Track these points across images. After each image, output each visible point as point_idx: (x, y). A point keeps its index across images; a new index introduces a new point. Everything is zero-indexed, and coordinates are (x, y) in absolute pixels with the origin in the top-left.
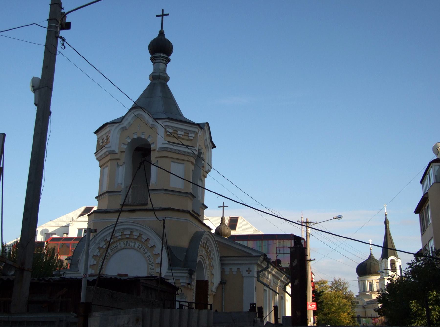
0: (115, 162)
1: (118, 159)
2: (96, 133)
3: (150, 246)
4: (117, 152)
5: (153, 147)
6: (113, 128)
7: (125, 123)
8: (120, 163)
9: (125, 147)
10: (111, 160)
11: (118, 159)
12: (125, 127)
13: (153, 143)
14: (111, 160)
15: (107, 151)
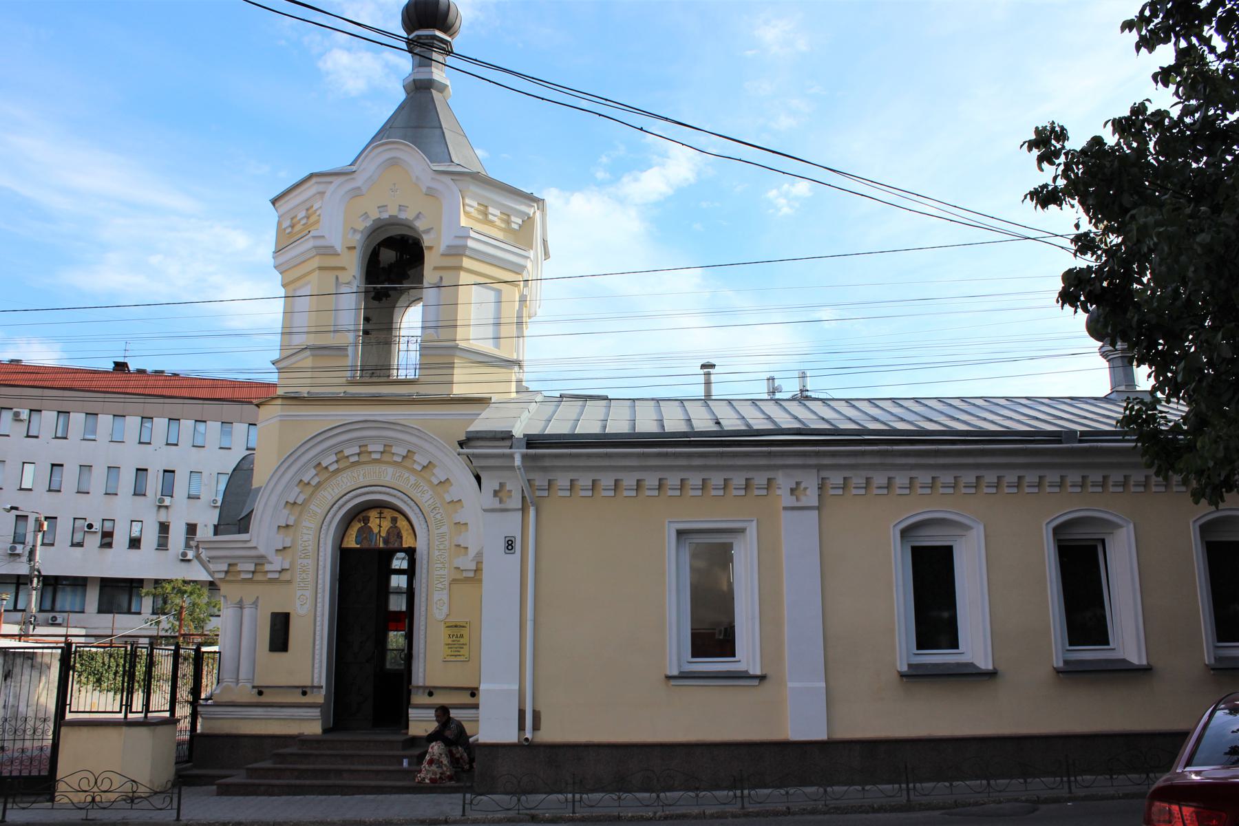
0: (331, 276)
1: (343, 269)
2: (274, 202)
3: (436, 482)
4: (339, 249)
5: (427, 241)
6: (332, 188)
7: (359, 181)
8: (345, 277)
9: (358, 237)
10: (320, 268)
11: (343, 269)
12: (359, 188)
13: (428, 231)
14: (320, 268)
15: (315, 247)
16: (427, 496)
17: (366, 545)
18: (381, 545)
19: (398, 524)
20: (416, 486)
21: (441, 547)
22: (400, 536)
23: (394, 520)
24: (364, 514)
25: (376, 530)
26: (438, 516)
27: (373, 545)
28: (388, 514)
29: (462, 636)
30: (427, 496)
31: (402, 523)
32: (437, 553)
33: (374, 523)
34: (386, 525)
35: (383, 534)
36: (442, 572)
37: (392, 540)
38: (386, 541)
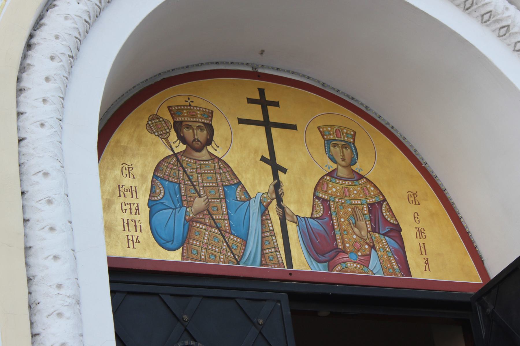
17: (212, 254)
18: (302, 262)
19: (362, 165)
24: (177, 96)
25: (257, 182)
27: (251, 260)
35: (300, 202)
37: (352, 234)
38: (322, 245)
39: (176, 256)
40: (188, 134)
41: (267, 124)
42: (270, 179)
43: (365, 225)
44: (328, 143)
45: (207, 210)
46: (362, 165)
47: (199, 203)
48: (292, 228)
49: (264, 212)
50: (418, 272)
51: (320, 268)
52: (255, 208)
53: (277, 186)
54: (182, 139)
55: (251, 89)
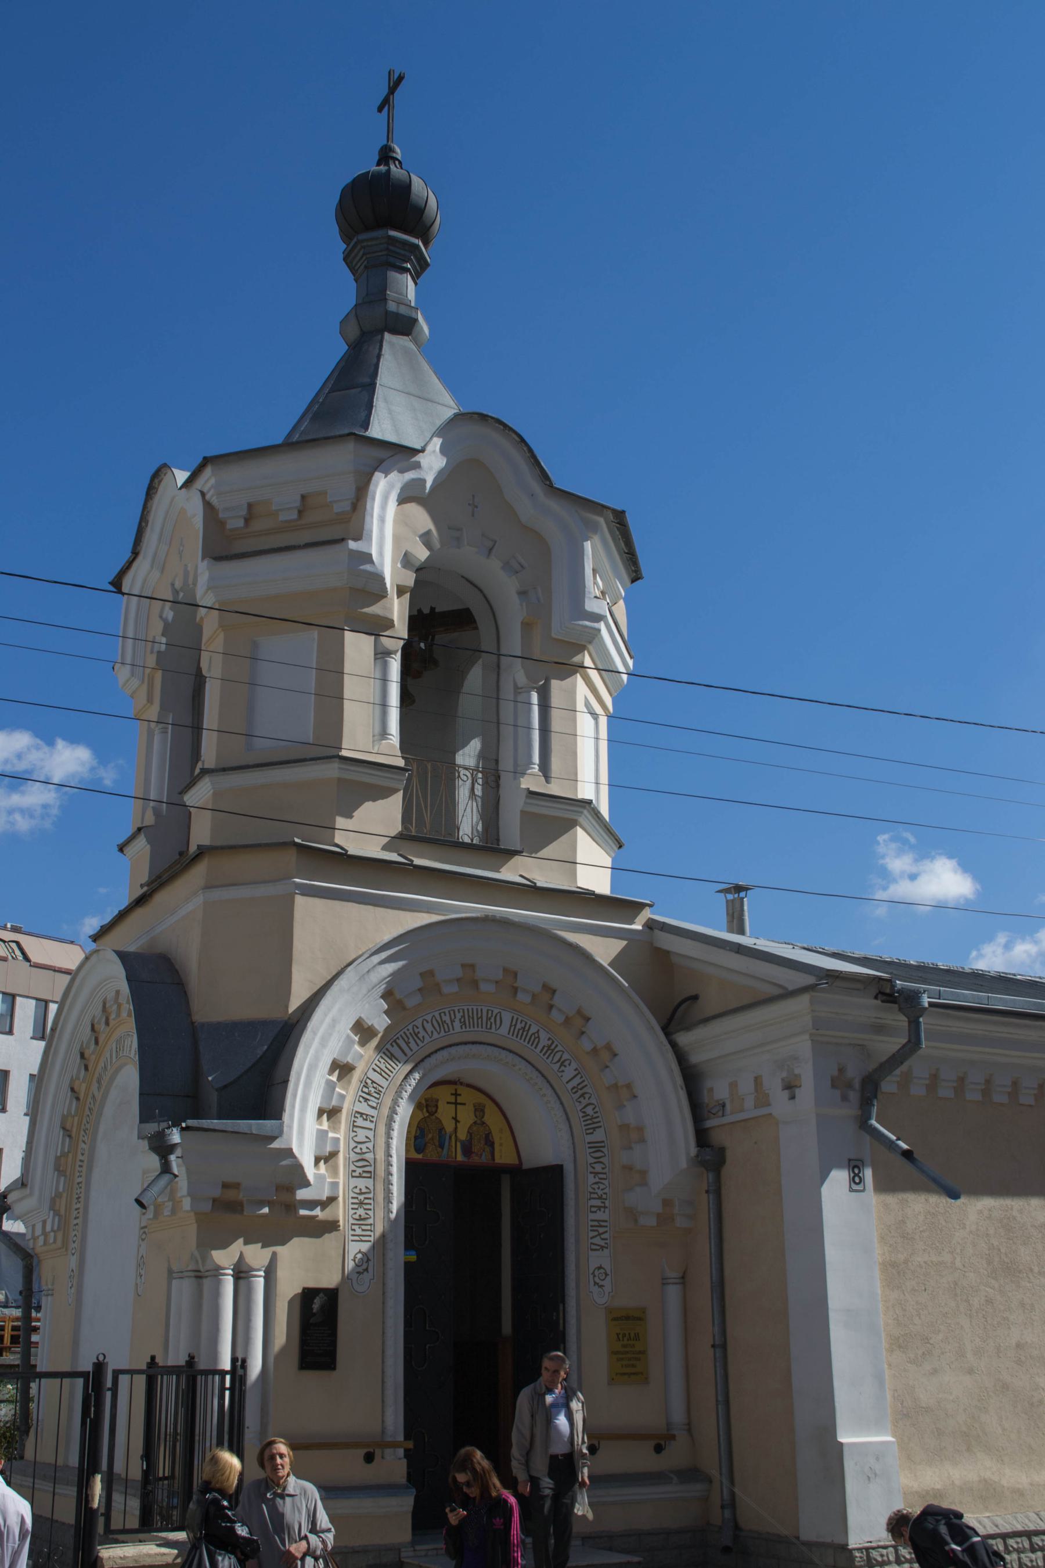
16: (569, 1072)
18: (460, 1157)
19: (485, 1119)
20: (550, 1050)
21: (598, 1168)
22: (490, 1142)
23: (479, 1110)
25: (449, 1126)
26: (589, 1110)
28: (467, 1096)
29: (637, 1337)
30: (569, 1072)
31: (492, 1118)
32: (591, 1179)
33: (445, 1113)
34: (467, 1117)
35: (462, 1135)
36: (600, 1215)
38: (467, 1150)
39: (420, 1156)
40: (430, 1109)
41: (456, 1103)
42: (454, 1126)
43: (483, 1142)
44: (476, 1110)
45: (432, 1139)
46: (485, 1119)
47: (430, 1136)
48: (459, 1144)
49: (450, 1138)
50: (498, 1160)
51: (465, 1159)
52: (447, 1138)
53: (456, 1128)
54: (427, 1111)
55: (451, 1089)
